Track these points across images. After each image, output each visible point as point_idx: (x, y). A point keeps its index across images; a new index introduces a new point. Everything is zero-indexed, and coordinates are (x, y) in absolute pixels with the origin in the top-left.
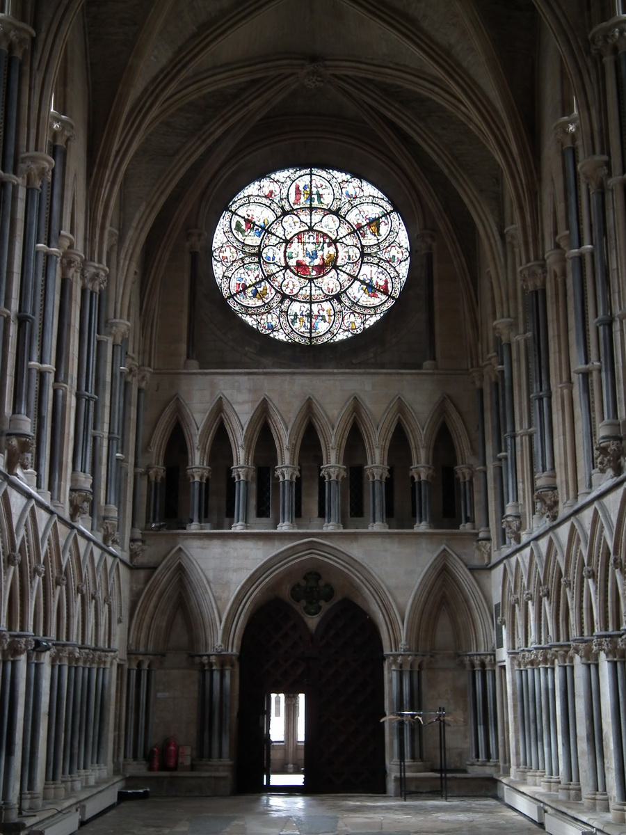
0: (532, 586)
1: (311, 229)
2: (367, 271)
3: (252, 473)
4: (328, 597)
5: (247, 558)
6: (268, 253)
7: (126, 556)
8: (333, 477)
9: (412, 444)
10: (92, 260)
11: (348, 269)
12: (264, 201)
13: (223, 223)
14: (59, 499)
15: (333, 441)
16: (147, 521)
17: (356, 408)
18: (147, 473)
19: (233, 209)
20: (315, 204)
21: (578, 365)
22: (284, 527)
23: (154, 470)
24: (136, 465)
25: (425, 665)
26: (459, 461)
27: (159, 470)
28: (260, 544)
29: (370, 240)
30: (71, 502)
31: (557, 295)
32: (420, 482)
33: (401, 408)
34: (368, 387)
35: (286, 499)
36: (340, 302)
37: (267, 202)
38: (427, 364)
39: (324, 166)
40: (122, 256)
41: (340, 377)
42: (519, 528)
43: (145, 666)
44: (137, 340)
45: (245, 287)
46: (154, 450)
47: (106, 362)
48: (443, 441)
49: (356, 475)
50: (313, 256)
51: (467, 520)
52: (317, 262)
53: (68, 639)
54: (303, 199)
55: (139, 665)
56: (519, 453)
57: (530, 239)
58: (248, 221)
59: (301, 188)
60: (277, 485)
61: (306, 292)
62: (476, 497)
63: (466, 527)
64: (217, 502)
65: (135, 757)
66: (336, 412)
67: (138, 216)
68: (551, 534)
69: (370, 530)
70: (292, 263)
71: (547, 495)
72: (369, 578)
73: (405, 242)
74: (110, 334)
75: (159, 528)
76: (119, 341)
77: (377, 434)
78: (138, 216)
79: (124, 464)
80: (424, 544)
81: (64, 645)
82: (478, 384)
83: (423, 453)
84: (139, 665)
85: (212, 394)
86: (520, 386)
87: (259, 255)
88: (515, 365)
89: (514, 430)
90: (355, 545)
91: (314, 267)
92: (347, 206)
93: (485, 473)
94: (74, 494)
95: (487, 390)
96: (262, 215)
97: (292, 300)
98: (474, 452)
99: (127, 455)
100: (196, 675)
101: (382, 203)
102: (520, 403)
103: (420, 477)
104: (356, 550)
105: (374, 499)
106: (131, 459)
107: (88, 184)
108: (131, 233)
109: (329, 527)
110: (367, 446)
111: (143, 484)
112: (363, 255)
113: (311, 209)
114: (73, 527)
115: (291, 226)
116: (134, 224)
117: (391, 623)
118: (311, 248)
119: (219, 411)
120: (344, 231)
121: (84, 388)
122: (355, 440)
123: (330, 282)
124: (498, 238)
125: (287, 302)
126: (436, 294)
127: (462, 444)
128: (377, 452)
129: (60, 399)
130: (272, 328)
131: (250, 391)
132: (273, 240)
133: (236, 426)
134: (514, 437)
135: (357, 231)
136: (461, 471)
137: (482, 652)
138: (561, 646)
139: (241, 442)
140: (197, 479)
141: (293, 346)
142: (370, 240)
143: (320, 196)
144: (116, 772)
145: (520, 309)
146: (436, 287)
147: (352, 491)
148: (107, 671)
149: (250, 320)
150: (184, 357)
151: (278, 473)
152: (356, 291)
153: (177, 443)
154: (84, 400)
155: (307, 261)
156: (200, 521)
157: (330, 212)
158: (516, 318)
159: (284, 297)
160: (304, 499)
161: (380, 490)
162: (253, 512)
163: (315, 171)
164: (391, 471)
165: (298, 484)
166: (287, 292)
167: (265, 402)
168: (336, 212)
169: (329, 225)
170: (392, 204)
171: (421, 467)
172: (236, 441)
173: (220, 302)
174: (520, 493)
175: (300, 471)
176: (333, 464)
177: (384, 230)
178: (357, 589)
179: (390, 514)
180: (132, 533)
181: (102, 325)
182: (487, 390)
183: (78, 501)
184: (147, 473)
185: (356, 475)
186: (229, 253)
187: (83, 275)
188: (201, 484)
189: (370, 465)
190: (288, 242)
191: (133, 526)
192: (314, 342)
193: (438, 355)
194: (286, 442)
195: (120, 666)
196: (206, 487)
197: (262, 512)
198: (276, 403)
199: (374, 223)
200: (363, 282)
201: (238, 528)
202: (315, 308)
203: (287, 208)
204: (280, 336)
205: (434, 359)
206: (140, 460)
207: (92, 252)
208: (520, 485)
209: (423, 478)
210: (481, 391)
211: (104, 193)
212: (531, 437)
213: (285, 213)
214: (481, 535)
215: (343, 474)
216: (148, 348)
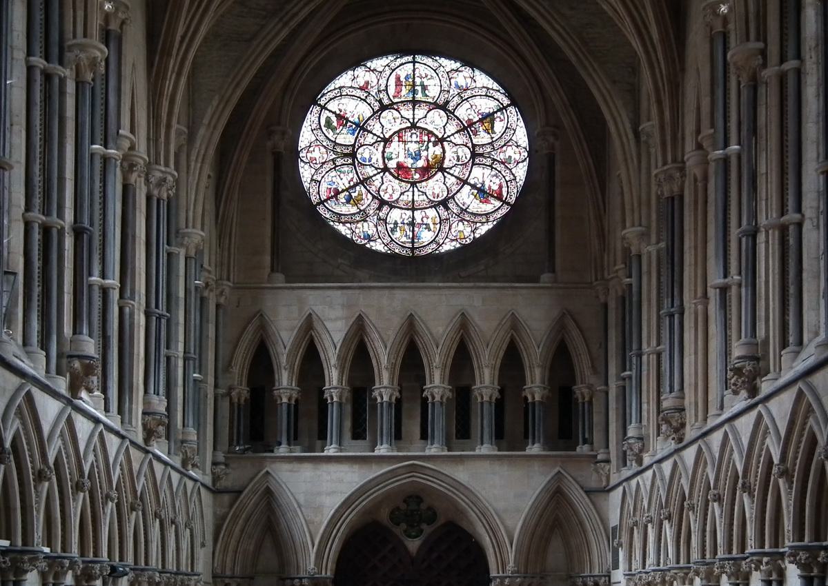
1: (414, 126)
3: (346, 394)
6: (363, 153)
8: (437, 398)
12: (359, 93)
15: (437, 360)
16: (230, 445)
18: (229, 394)
20: (419, 96)
21: (715, 279)
23: (237, 391)
24: (216, 386)
26: (578, 379)
28: (356, 467)
31: (696, 202)
32: (533, 403)
35: (385, 421)
37: (362, 94)
49: (462, 396)
50: (417, 157)
51: (585, 442)
52: (421, 163)
54: (404, 91)
56: (644, 373)
59: (402, 79)
62: (596, 418)
63: (583, 449)
64: (308, 425)
69: (477, 452)
77: (487, 353)
79: (202, 385)
86: (649, 301)
89: (640, 348)
93: (607, 393)
98: (594, 368)
99: (206, 375)
103: (534, 398)
106: (211, 380)
110: (475, 365)
111: (225, 405)
113: (415, 103)
115: (390, 122)
118: (413, 147)
119: (308, 327)
121: (153, 305)
122: (462, 359)
128: (487, 372)
129: (127, 317)
132: (370, 139)
134: (640, 356)
136: (580, 391)
139: (333, 361)
140: (285, 400)
143: (424, 88)
151: (376, 393)
153: (262, 363)
154: (154, 318)
155: (409, 162)
157: (436, 106)
160: (404, 421)
161: (488, 412)
162: (347, 434)
164: (501, 391)
165: (398, 406)
168: (444, 107)
169: (435, 122)
171: (535, 386)
172: (328, 360)
175: (400, 392)
176: (437, 384)
180: (214, 456)
184: (229, 394)
185: (462, 396)
188: (289, 405)
189: (478, 385)
190: (387, 141)
191: (215, 448)
194: (384, 360)
196: (295, 410)
197: (358, 434)
198: (372, 318)
203: (386, 102)
209: (537, 398)
212: (659, 355)
213: (383, 108)
215: (449, 394)
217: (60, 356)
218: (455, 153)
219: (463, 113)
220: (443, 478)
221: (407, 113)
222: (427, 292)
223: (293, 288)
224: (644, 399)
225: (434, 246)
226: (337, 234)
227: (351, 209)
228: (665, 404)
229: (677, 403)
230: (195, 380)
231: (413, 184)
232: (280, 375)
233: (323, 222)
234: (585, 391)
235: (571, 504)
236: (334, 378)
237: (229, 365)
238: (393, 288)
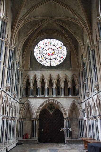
0: (92, 105)
2: (60, 55)
3: (41, 87)
4: (54, 109)
5: (40, 102)
6: (43, 52)
7: (19, 101)
9: (68, 82)
10: (11, 44)
11: (57, 54)
14: (3, 87)
15: (55, 82)
17: (58, 76)
18: (23, 87)
19: (38, 45)
22: (46, 96)
25: (71, 120)
27: (25, 87)
29: (60, 50)
30: (6, 88)
33: (66, 76)
34: (60, 72)
35: (47, 91)
37: (43, 44)
38: (70, 69)
39: (52, 38)
41: (55, 71)
42: (89, 95)
43: (22, 121)
44: (21, 65)
47: (15, 66)
48: (73, 82)
49: (58, 88)
52: (52, 53)
53: (5, 115)
55: (21, 120)
56: (88, 82)
57: (91, 41)
58: (40, 47)
60: (45, 90)
61: (50, 58)
63: (77, 96)
64: (35, 92)
65: (20, 137)
67: (21, 42)
68: (98, 94)
69: (61, 97)
70: (47, 53)
71: (97, 87)
72: (61, 105)
73: (66, 50)
74: (16, 61)
76: (17, 62)
78: (21, 42)
80: (70, 99)
81: (5, 116)
82: (79, 72)
83: (70, 83)
84: (21, 120)
85: (34, 74)
86: (88, 70)
87: (42, 52)
88: (87, 66)
90: (59, 99)
92: (56, 45)
94: (7, 87)
95: (81, 73)
96: (43, 46)
98: (79, 83)
99: (19, 84)
100: (31, 122)
101: (62, 44)
102: (88, 73)
104: (59, 100)
105: (62, 92)
106: (20, 85)
107: (11, 32)
108: (20, 44)
109: (55, 96)
111: (22, 89)
112: (59, 52)
113: (50, 45)
114: (6, 93)
115: (47, 48)
116: (21, 43)
117: (65, 113)
119: (35, 77)
120: (56, 48)
122: (58, 82)
123: (54, 56)
124: (83, 45)
125: (46, 59)
126: (71, 57)
127: (77, 82)
128: (62, 83)
129: (4, 68)
132: (44, 50)
133: (38, 79)
134: (87, 79)
135: (58, 48)
136: (76, 86)
137: (81, 117)
138: (100, 116)
139: (39, 82)
140: (31, 88)
141: (48, 66)
142: (60, 50)
144: (17, 140)
145: (88, 57)
146: (71, 56)
147: (58, 91)
148: (15, 122)
149: (41, 63)
151: (45, 87)
152: (58, 58)
153: (28, 82)
158: (87, 58)
159: (46, 59)
162: (41, 94)
163: (51, 39)
168: (54, 46)
169: (53, 47)
170: (64, 44)
171: (70, 86)
172: (38, 82)
174: (89, 88)
176: (55, 85)
177: (62, 48)
178: (59, 107)
179: (64, 94)
180: (20, 97)
181: (14, 60)
182: (81, 73)
183: (7, 88)
184: (23, 87)
185: (58, 88)
187: (10, 47)
190: (46, 50)
191: (20, 96)
192: (51, 66)
193: (72, 67)
195: (17, 120)
196: (33, 90)
197: (42, 94)
198: (45, 75)
201: (38, 96)
202: (51, 60)
204: (45, 65)
205: (71, 68)
206: (21, 85)
207: (12, 43)
208: (89, 87)
210: (79, 73)
211: (14, 33)
212: (90, 78)
213: (46, 46)
214: (80, 97)
215: (56, 87)
218: (56, 52)
219: (57, 46)
220: (55, 101)
221: (49, 46)
222: (53, 71)
223: (33, 70)
224: (89, 86)
225: (54, 65)
226: (39, 63)
227: (41, 59)
230: (17, 84)
231: (50, 56)
233: (37, 61)
234: (77, 87)
235: (76, 105)
236: (39, 85)
237: (23, 83)
238: (48, 70)
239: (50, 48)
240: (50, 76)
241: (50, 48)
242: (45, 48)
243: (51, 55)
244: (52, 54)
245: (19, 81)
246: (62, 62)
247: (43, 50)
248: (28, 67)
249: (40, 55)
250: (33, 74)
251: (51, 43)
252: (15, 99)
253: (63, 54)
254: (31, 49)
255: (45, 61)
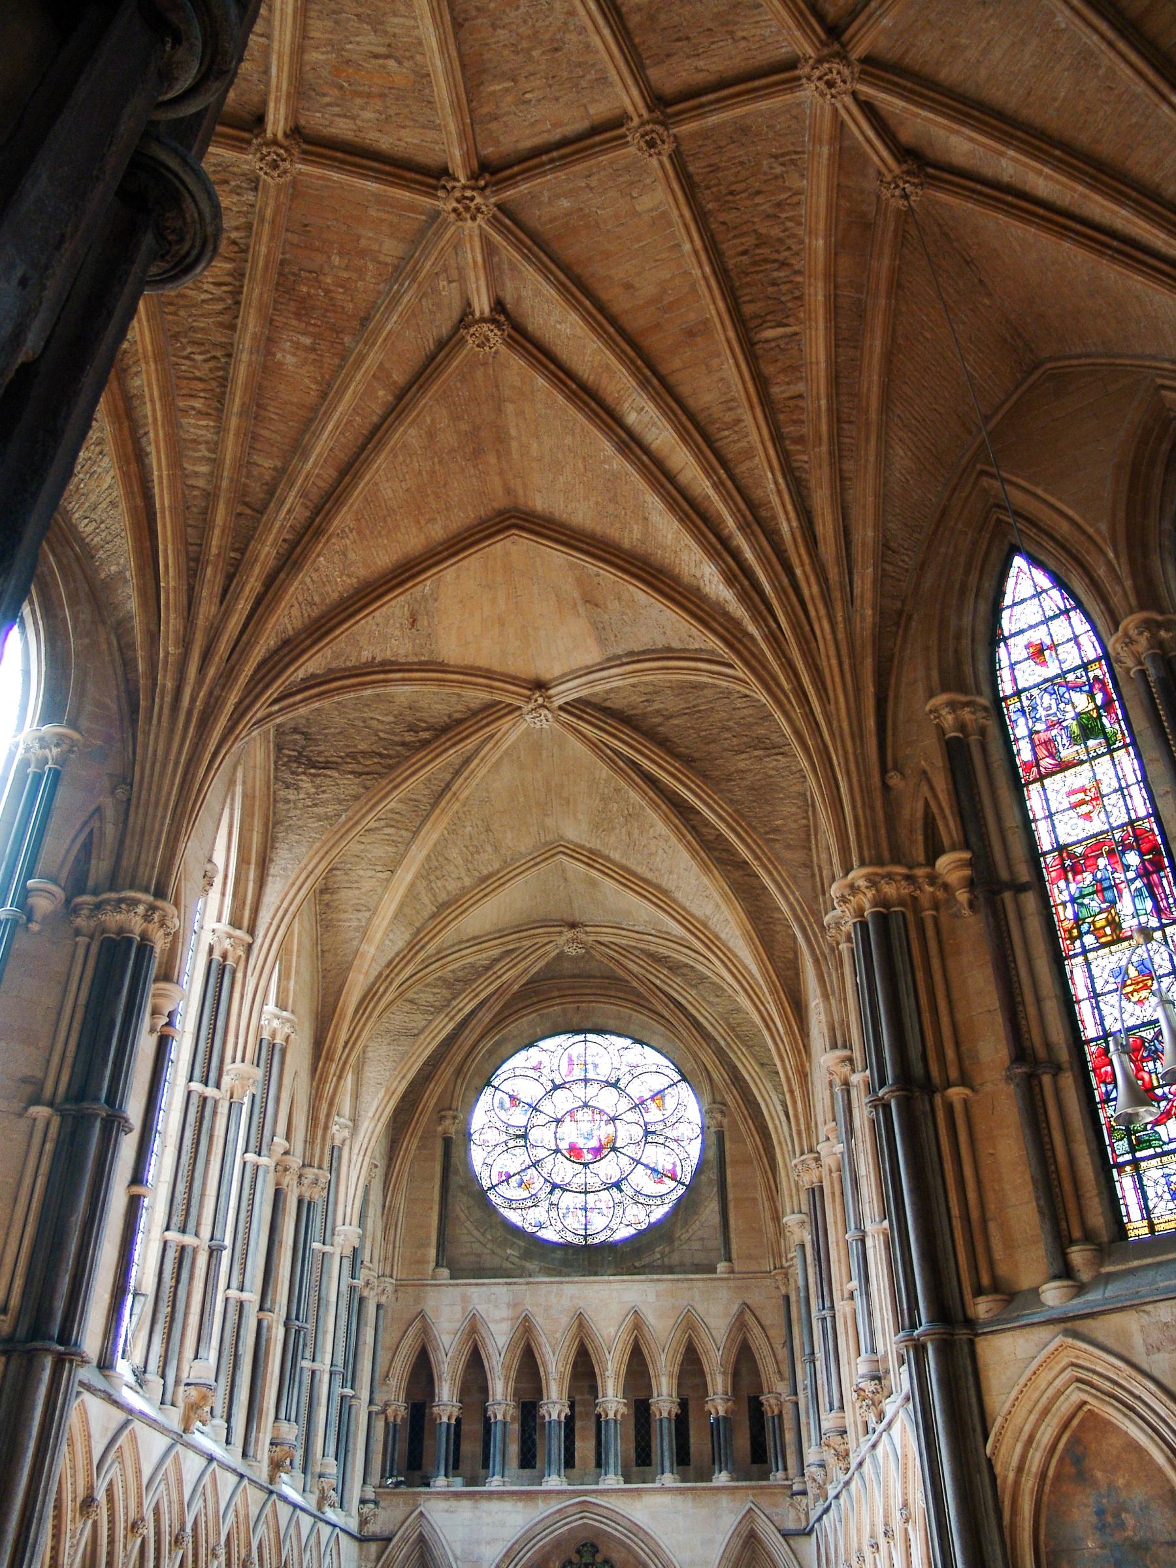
3: (511, 1411)
6: (534, 1135)
8: (611, 1415)
9: (706, 1369)
11: (630, 1151)
12: (531, 1073)
13: (486, 1098)
17: (638, 1325)
18: (384, 1411)
19: (495, 1084)
20: (590, 1076)
24: (371, 1402)
26: (766, 1390)
27: (399, 1409)
34: (651, 1298)
36: (621, 1191)
39: (600, 1031)
40: (355, 1151)
41: (617, 1286)
45: (509, 1176)
46: (393, 1382)
50: (589, 1137)
52: (594, 1143)
58: (513, 1098)
61: (580, 1180)
66: (612, 1330)
75: (397, 1484)
77: (663, 1357)
79: (354, 1402)
83: (719, 1379)
85: (464, 1309)
87: (524, 1137)
91: (589, 1150)
93: (797, 1404)
96: (530, 1091)
97: (564, 1190)
105: (663, 1445)
106: (365, 1395)
111: (380, 1425)
112: (647, 1133)
113: (586, 1081)
115: (562, 1101)
116: (371, 1114)
118: (585, 1127)
120: (624, 1104)
123: (609, 1168)
125: (557, 1192)
128: (664, 1380)
130: (541, 1226)
131: (509, 1305)
132: (541, 1119)
133: (492, 1350)
135: (639, 1106)
140: (445, 1419)
141: (567, 1246)
142: (654, 1114)
143: (596, 1066)
146: (728, 1172)
150: (432, 1265)
151: (543, 1411)
152: (641, 1179)
155: (581, 1143)
156: (446, 1476)
157: (608, 1084)
159: (555, 1186)
163: (590, 1037)
164: (683, 1404)
165: (570, 1421)
166: (558, 1181)
167: (526, 1319)
168: (615, 1085)
169: (607, 1100)
172: (492, 1369)
173: (481, 1197)
177: (670, 1102)
179: (682, 1458)
184: (384, 1411)
186: (492, 1137)
188: (449, 1425)
190: (558, 1121)
192: (590, 1241)
193: (734, 1255)
198: (539, 1321)
199: (659, 1096)
200: (647, 1166)
202: (591, 1198)
204: (549, 1235)
205: (729, 1260)
206: (377, 1396)
210: (787, 1298)
213: (556, 1087)
216: (390, 1254)
217: (177, 1382)
219: (637, 1090)
221: (578, 1089)
228: (825, 1425)
229: (839, 1422)
230: (343, 1397)
232: (440, 1389)
236: (500, 1389)
239: (586, 1105)
240: (581, 1325)
241: (586, 1105)
242: (546, 1106)
243: (588, 1157)
244: (597, 1151)
245: (359, 1367)
246: (665, 1209)
247: (535, 1121)
248: (422, 1261)
249: (514, 1161)
250: (459, 1316)
251: (590, 1067)
252: (331, 1514)
253: (674, 1145)
254: (448, 1122)
255: (545, 1205)
